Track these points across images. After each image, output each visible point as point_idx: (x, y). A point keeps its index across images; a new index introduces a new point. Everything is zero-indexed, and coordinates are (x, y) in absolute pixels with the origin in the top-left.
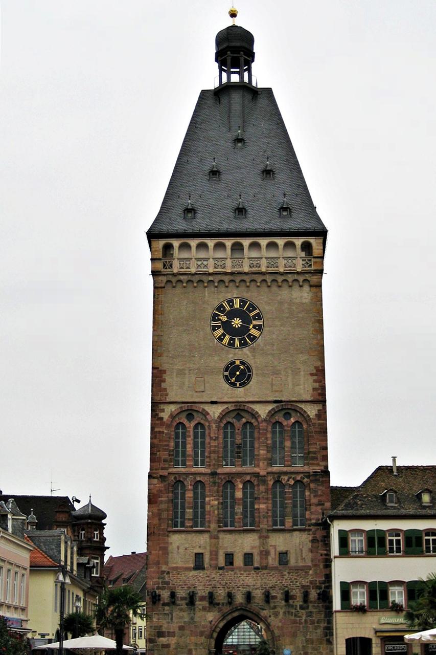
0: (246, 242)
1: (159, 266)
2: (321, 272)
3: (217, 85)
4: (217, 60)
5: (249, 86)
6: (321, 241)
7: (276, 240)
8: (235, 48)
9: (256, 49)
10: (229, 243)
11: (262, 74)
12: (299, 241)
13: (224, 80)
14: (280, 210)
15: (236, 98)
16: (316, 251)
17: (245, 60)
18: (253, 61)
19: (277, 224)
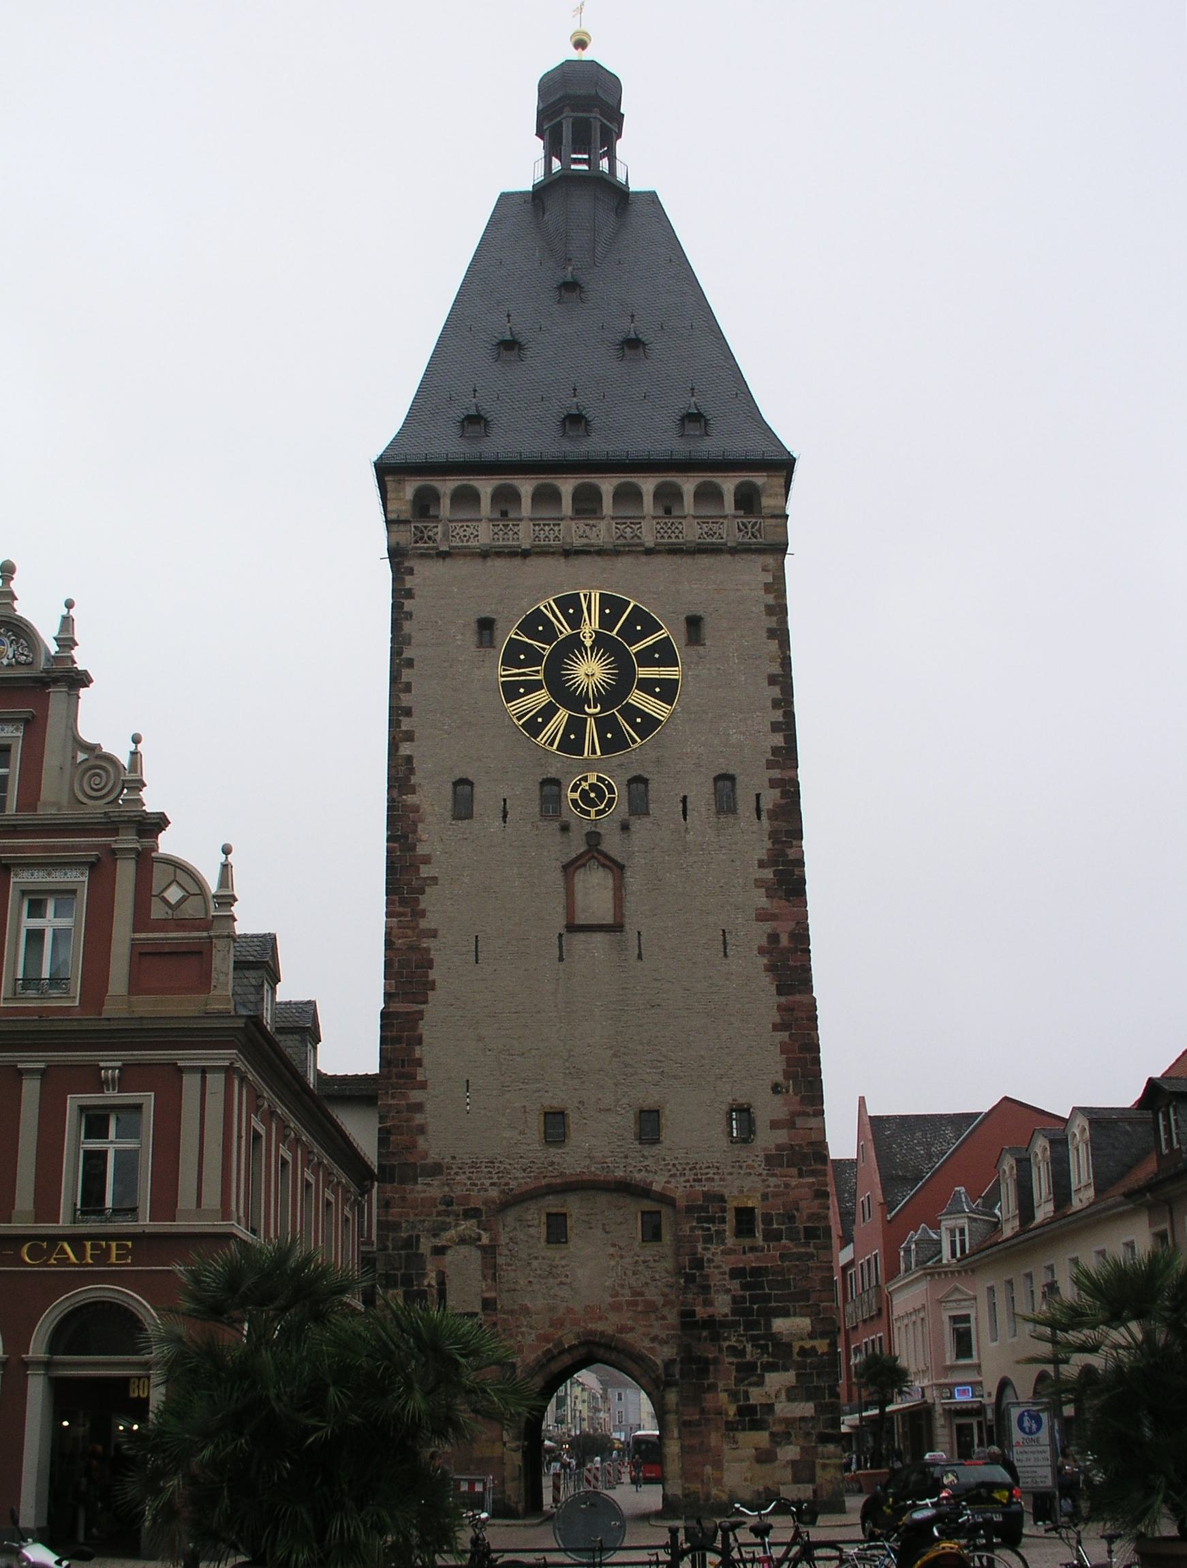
0: (607, 485)
1: (406, 536)
2: (780, 549)
3: (539, 176)
4: (540, 133)
5: (610, 178)
6: (782, 481)
7: (674, 479)
8: (580, 108)
9: (626, 107)
10: (567, 486)
11: (637, 161)
12: (728, 484)
13: (556, 165)
14: (683, 419)
15: (582, 203)
16: (766, 502)
17: (603, 126)
18: (619, 136)
19: (678, 447)
